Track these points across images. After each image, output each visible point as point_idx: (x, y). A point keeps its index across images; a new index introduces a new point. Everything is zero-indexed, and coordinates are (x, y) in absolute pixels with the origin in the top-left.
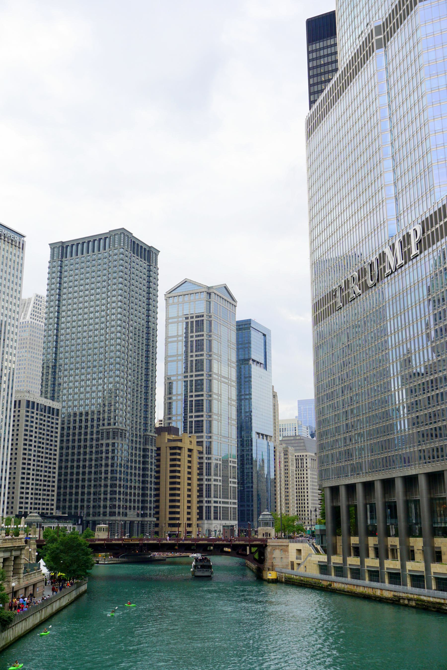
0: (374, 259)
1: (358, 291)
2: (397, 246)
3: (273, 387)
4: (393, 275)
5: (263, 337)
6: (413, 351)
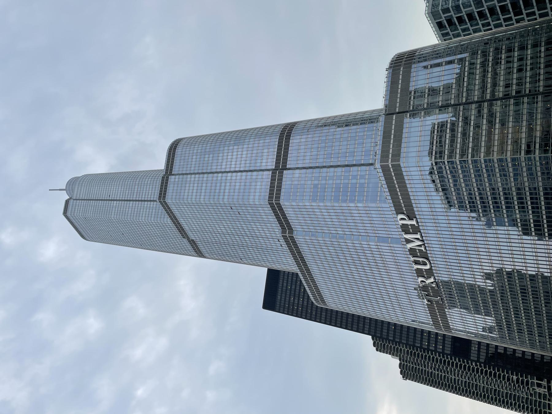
0: (412, 259)
1: (432, 280)
2: (408, 236)
4: (426, 245)
6: (485, 326)
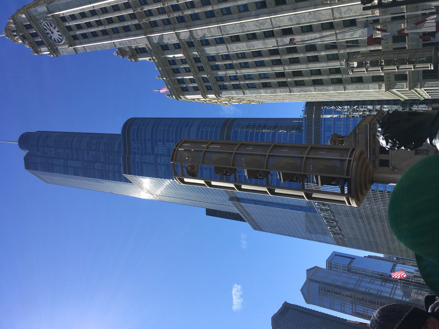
3: (365, 257)
5: (337, 257)
